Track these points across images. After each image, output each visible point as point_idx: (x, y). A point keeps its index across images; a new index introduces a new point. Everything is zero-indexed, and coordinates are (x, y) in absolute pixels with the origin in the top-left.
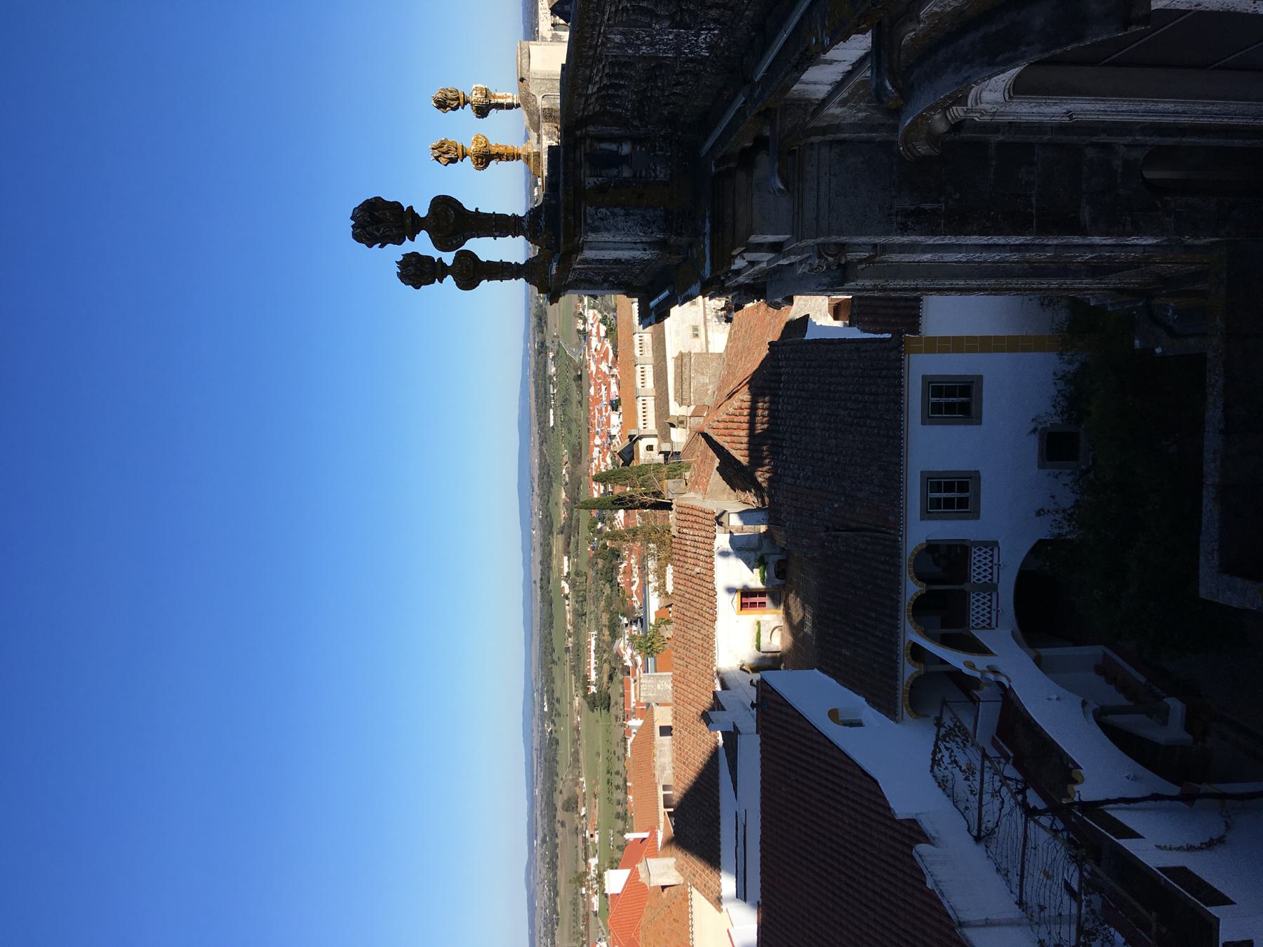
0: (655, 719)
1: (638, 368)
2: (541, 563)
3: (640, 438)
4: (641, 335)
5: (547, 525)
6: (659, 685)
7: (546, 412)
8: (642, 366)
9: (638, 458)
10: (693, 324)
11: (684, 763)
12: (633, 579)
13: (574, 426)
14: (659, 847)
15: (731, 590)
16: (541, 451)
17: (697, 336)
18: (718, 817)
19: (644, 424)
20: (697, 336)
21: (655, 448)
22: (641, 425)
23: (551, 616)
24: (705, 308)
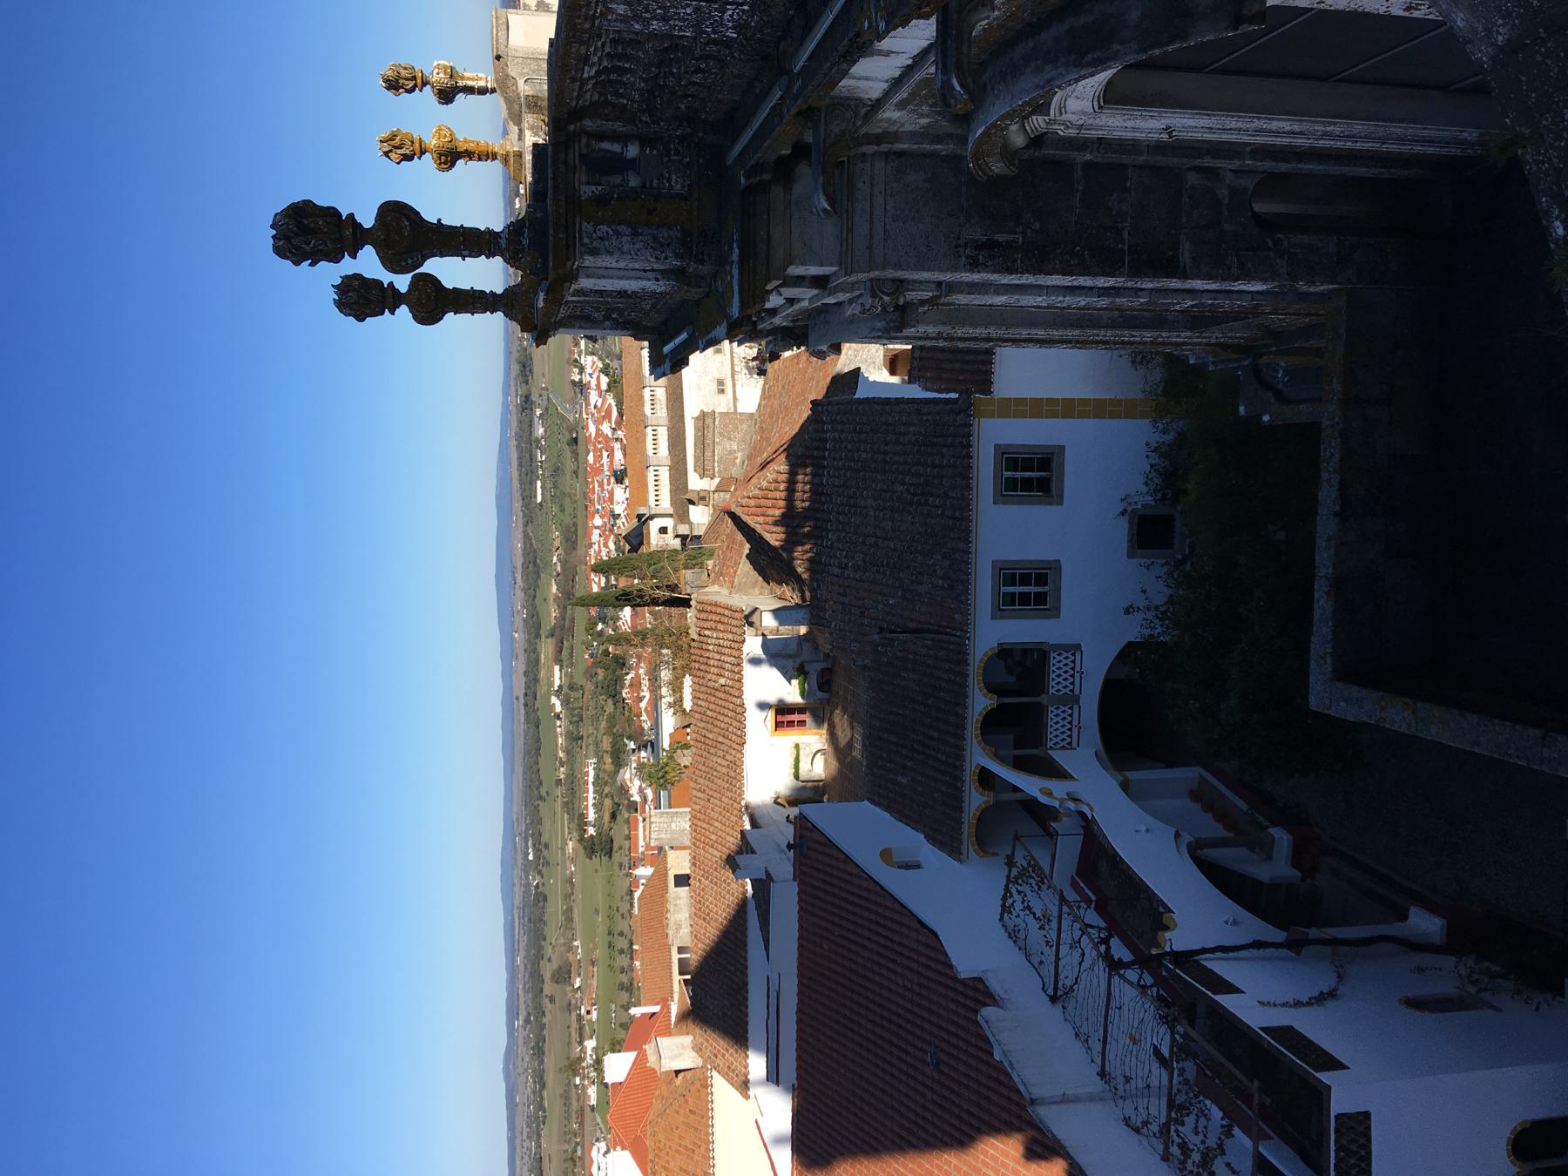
0: (669, 866)
1: (649, 430)
2: (526, 674)
3: (652, 517)
4: (652, 389)
5: (534, 627)
6: (673, 825)
7: (532, 484)
8: (654, 428)
9: (649, 543)
10: (718, 376)
11: (704, 919)
12: (642, 694)
13: (567, 502)
14: (673, 1023)
15: (763, 706)
16: (526, 535)
17: (722, 391)
18: (746, 984)
19: (657, 500)
20: (722, 391)
21: (670, 530)
22: (652, 502)
23: (538, 740)
24: (732, 357)
